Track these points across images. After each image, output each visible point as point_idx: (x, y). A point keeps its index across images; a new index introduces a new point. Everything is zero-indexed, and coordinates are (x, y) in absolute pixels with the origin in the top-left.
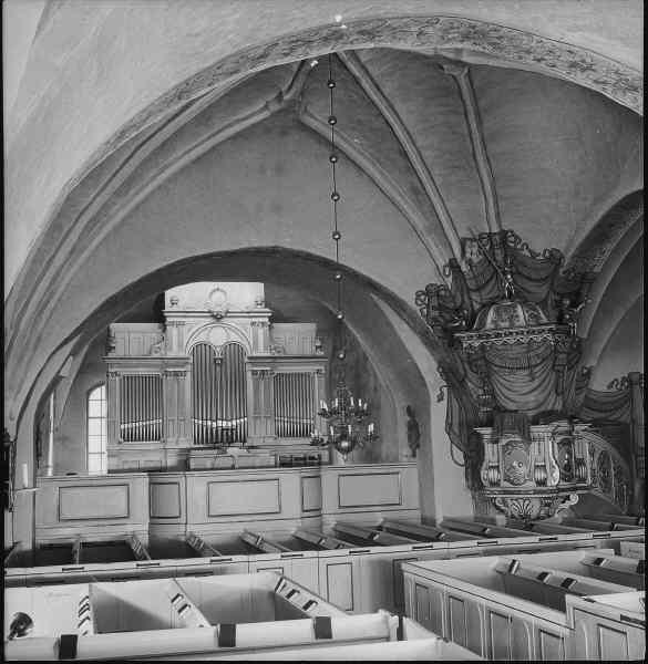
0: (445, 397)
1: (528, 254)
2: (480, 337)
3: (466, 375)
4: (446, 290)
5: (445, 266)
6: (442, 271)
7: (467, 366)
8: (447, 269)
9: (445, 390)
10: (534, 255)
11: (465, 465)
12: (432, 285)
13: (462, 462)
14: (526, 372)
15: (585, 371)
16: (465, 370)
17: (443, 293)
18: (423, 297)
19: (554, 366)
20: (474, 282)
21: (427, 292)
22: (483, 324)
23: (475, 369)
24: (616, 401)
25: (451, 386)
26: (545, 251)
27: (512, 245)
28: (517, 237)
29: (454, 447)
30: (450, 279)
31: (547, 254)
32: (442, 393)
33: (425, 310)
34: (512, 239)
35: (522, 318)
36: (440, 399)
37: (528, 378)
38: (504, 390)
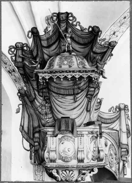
0: (21, 111)
1: (79, 29)
2: (51, 72)
3: (35, 98)
4: (27, 46)
5: (29, 32)
6: (27, 34)
7: (37, 93)
8: (30, 34)
9: (21, 106)
10: (82, 30)
11: (30, 150)
12: (20, 43)
13: (29, 149)
14: (72, 97)
15: (99, 101)
16: (35, 94)
17: (25, 48)
18: (13, 50)
19: (86, 96)
20: (46, 42)
21: (16, 47)
22: (51, 65)
23: (41, 94)
24: (113, 118)
25: (24, 104)
26: (90, 27)
27: (71, 22)
28: (74, 17)
29: (24, 139)
30: (32, 39)
31: (91, 29)
32: (19, 108)
33: (14, 58)
34: (71, 18)
35: (75, 63)
36: (18, 112)
37: (72, 101)
38: (57, 107)
